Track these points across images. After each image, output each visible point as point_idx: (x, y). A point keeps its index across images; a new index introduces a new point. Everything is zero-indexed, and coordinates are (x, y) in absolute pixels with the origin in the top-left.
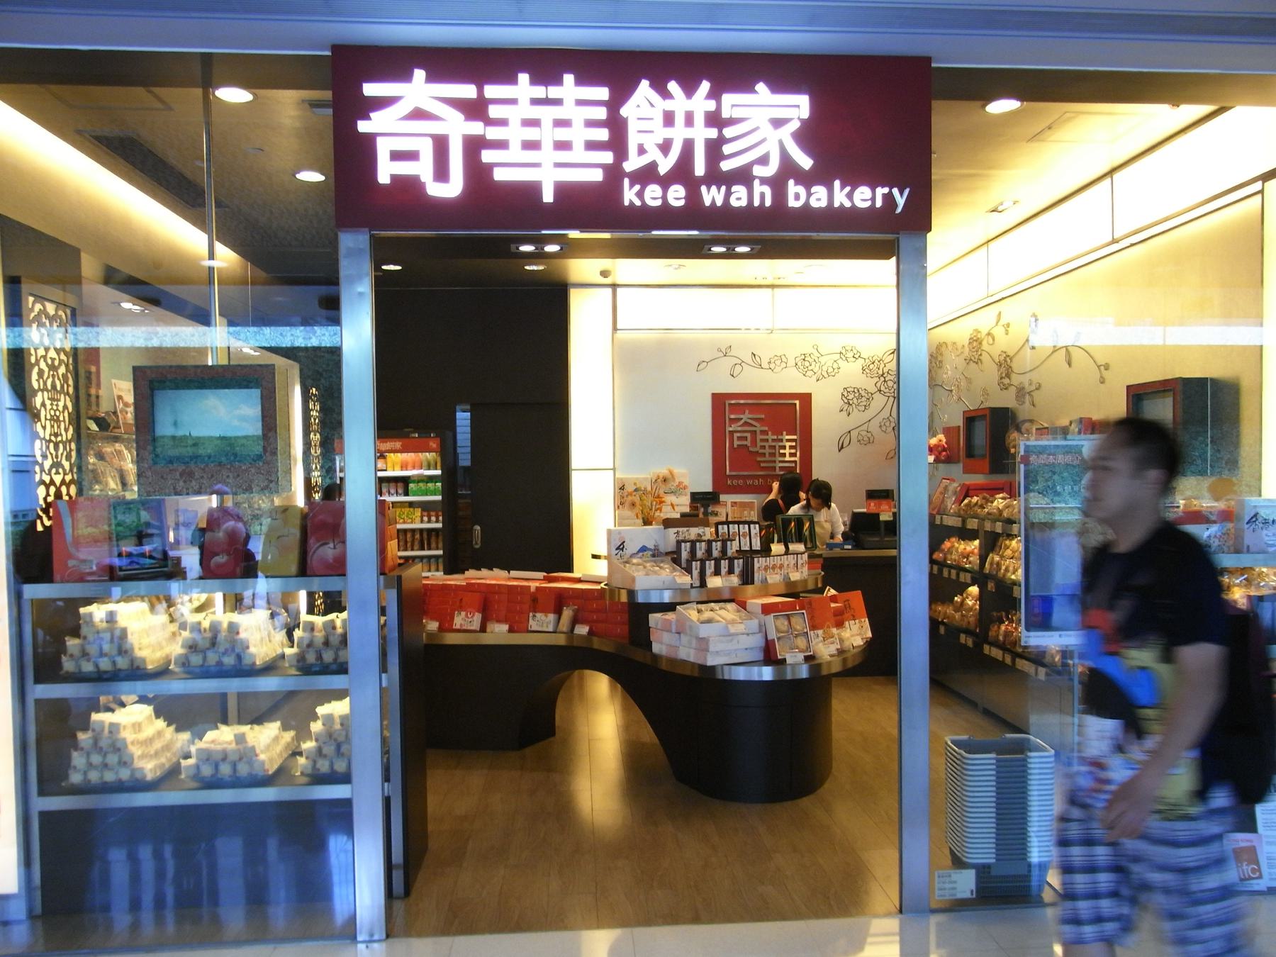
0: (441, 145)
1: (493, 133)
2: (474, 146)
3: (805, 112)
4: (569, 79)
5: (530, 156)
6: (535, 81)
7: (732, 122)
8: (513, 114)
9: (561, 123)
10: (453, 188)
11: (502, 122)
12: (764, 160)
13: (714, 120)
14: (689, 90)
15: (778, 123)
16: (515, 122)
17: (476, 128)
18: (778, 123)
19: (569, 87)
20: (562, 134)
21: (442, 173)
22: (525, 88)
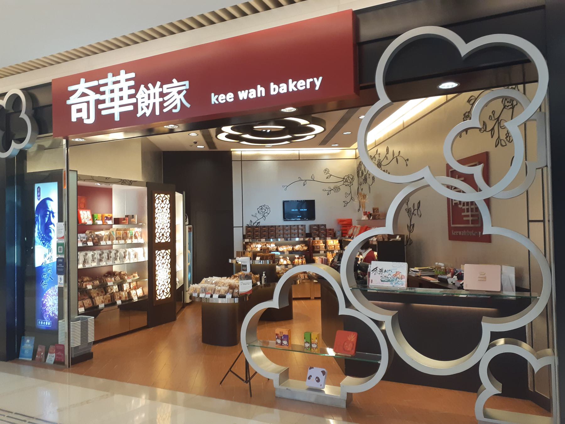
1: (101, 97)
2: (98, 102)
3: (187, 87)
11: (103, 93)
12: (175, 107)
16: (107, 92)
18: (179, 92)
19: (123, 76)
22: (110, 79)
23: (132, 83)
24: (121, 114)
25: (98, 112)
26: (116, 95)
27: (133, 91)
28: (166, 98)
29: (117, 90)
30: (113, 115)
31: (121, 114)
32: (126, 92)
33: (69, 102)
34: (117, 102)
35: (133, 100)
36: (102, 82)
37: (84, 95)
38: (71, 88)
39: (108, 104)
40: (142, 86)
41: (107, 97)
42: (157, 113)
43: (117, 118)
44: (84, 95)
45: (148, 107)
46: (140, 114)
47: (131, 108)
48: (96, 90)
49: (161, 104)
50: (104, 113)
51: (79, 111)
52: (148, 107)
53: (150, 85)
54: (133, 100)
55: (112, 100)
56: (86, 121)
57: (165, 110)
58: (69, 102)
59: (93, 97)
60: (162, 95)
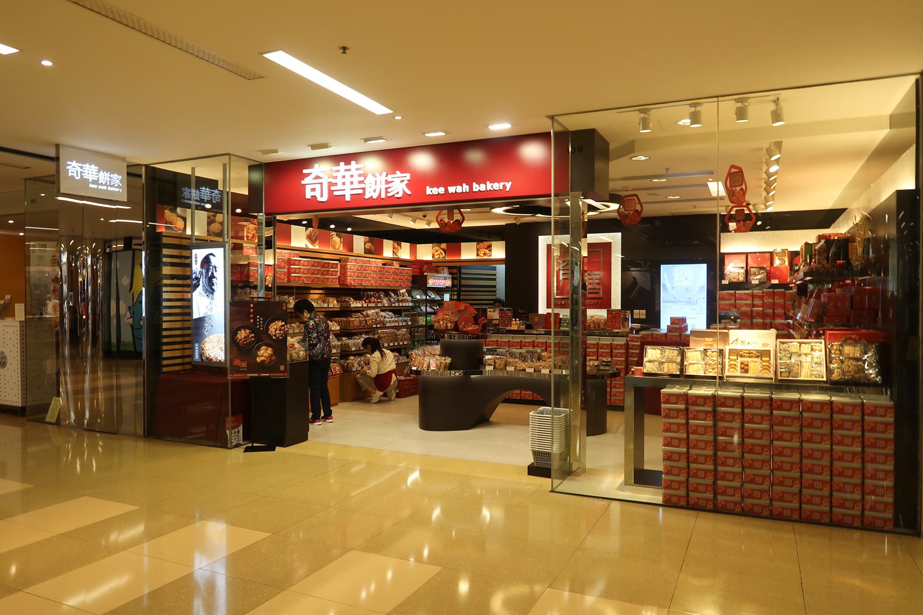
0: (77, 171)
1: (84, 171)
2: (81, 173)
4: (93, 165)
5: (88, 175)
6: (89, 165)
7: (112, 178)
8: (87, 169)
9: (92, 171)
10: (78, 178)
13: (110, 177)
14: (107, 173)
15: (118, 179)
17: (82, 170)
18: (118, 179)
20: (92, 173)
21: (77, 176)
23: (97, 171)
24: (92, 180)
25: (82, 176)
26: (91, 173)
27: (97, 173)
28: (112, 179)
29: (90, 171)
30: (89, 179)
31: (92, 180)
32: (94, 173)
33: (67, 168)
34: (90, 175)
35: (98, 177)
36: (84, 165)
37: (74, 167)
38: (68, 163)
39: (86, 174)
40: (102, 171)
41: (87, 172)
42: (108, 184)
43: (90, 181)
44: (74, 167)
45: (104, 180)
46: (99, 183)
47: (97, 179)
48: (81, 168)
49: (110, 181)
50: (84, 177)
51: (73, 173)
52: (104, 180)
53: (105, 172)
54: (98, 177)
55: (88, 174)
56: (76, 178)
57: (111, 184)
58: (67, 168)
59: (79, 170)
60: (110, 177)
